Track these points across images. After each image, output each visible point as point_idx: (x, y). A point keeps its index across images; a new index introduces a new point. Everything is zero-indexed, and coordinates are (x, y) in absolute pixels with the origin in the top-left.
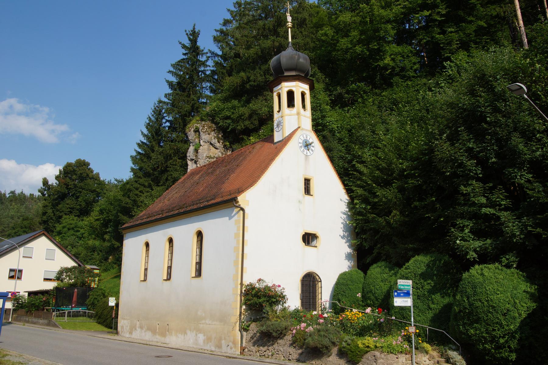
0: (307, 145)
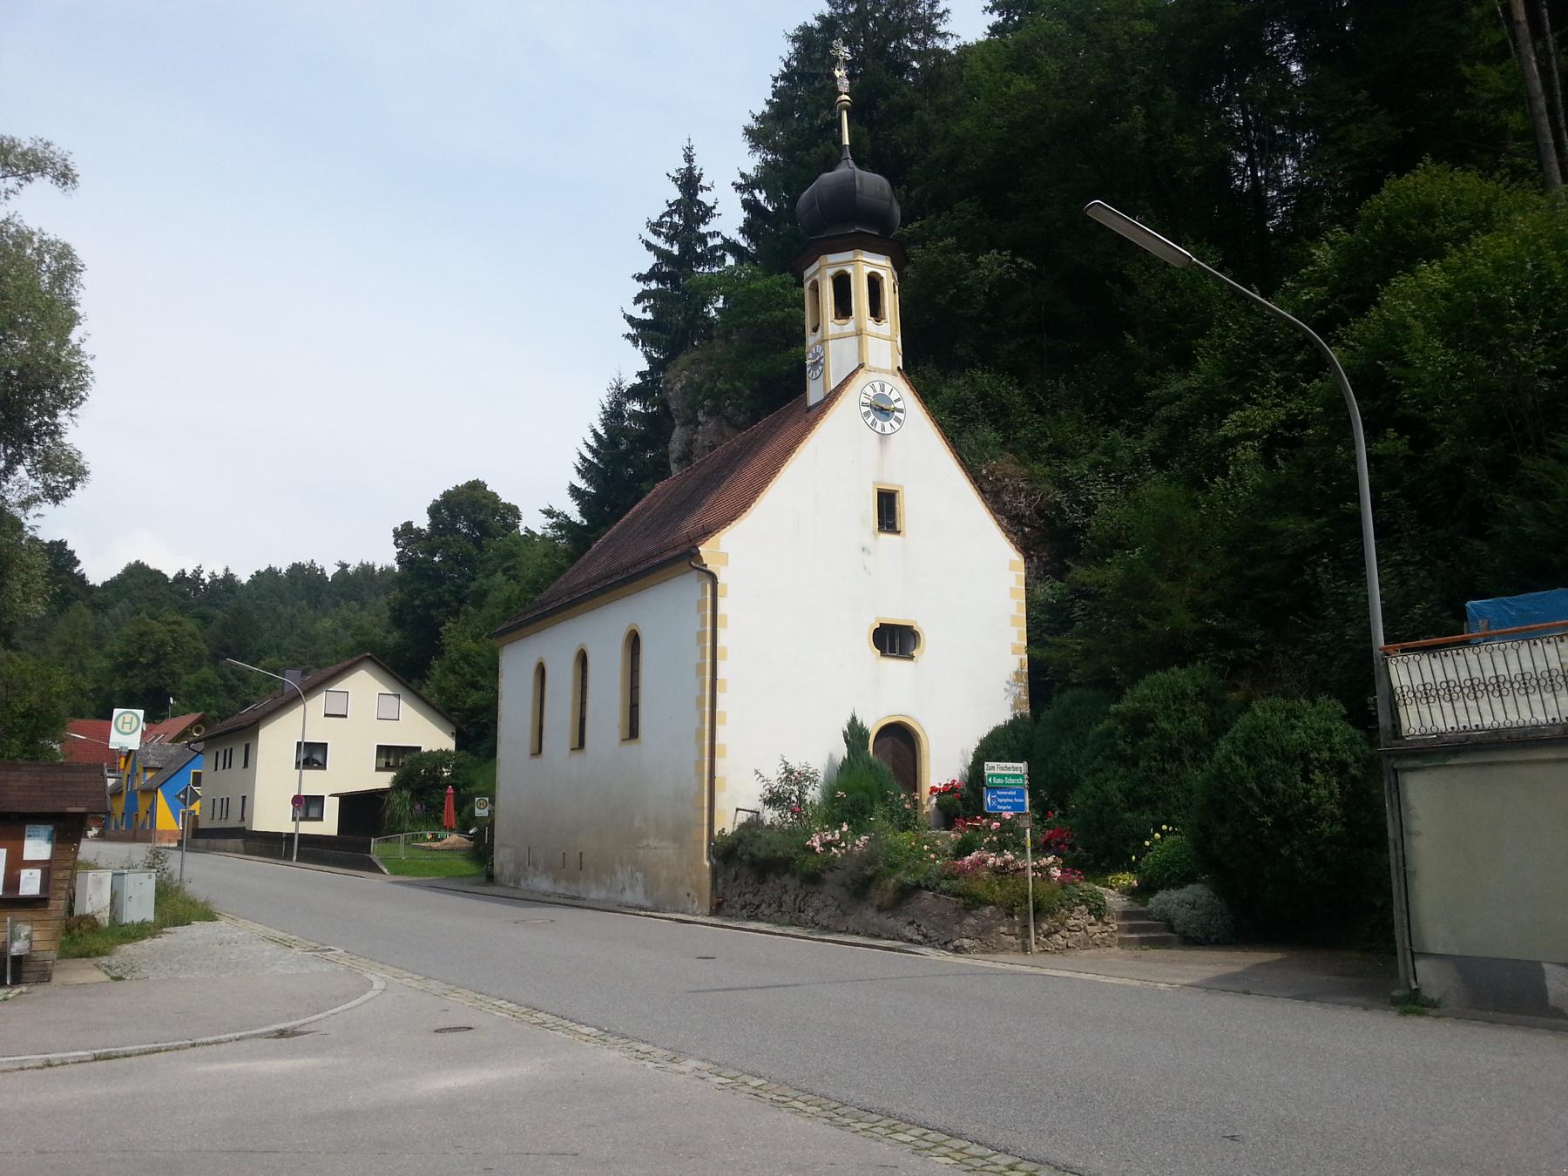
0: (882, 409)
